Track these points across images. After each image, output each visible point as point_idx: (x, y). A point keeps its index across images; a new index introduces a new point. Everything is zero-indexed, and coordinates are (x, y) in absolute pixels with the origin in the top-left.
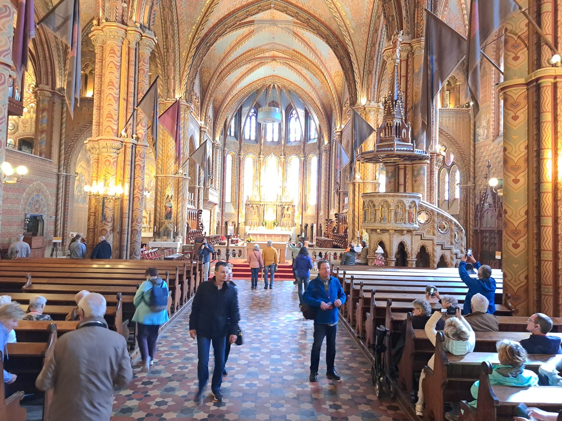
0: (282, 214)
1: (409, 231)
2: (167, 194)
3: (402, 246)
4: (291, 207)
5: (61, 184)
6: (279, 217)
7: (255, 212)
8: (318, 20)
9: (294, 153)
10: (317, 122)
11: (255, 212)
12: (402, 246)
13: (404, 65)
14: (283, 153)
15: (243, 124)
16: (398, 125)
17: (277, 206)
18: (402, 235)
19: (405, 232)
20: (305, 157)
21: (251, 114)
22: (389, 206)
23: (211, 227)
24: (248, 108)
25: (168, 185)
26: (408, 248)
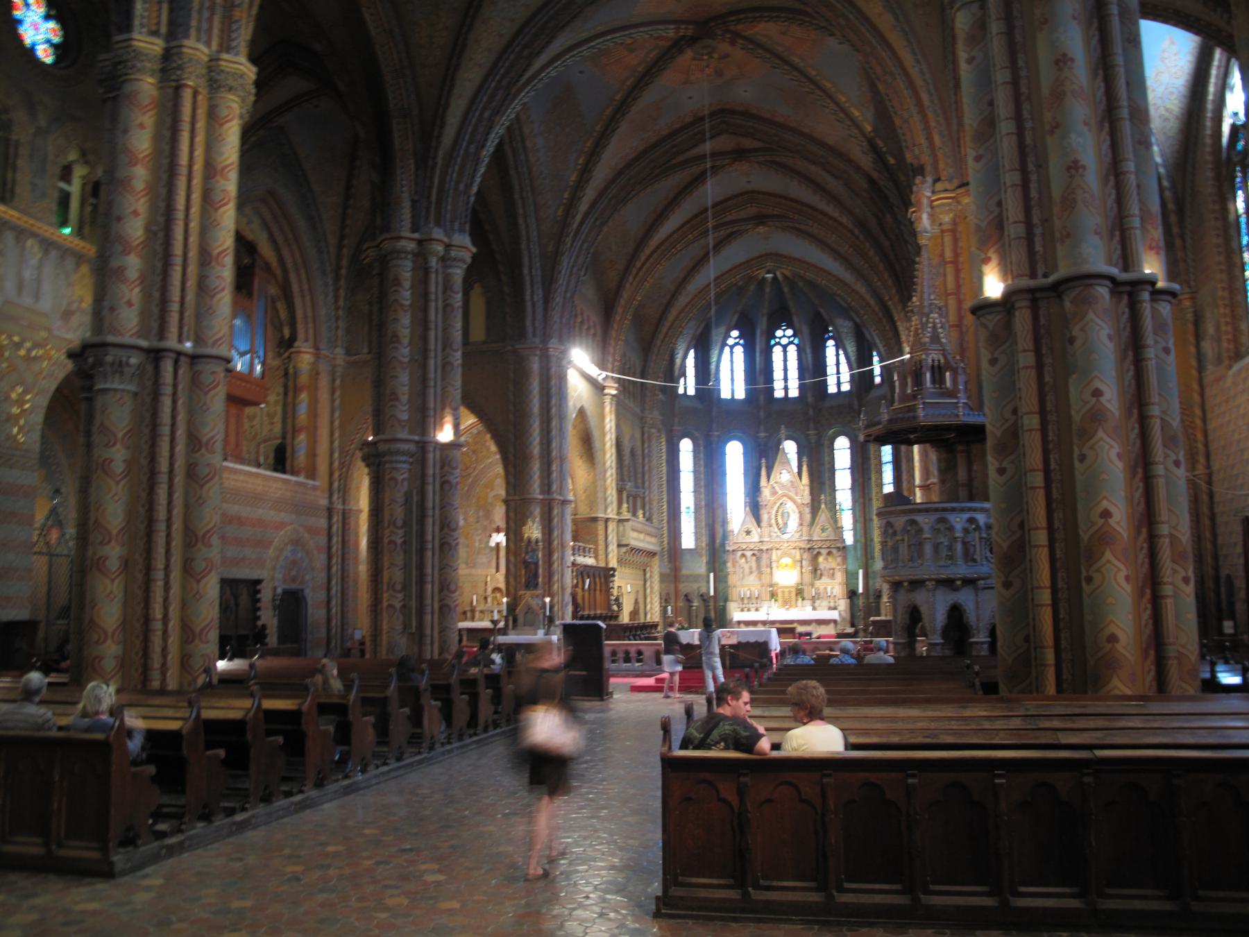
1: (969, 582)
2: (526, 536)
3: (956, 612)
4: (834, 551)
5: (334, 528)
6: (808, 577)
7: (751, 568)
8: (823, 144)
10: (882, 350)
12: (956, 612)
13: (948, 239)
15: (713, 367)
16: (936, 363)
18: (956, 589)
19: (959, 583)
21: (730, 342)
22: (920, 531)
23: (648, 607)
24: (722, 330)
25: (528, 518)
26: (971, 616)
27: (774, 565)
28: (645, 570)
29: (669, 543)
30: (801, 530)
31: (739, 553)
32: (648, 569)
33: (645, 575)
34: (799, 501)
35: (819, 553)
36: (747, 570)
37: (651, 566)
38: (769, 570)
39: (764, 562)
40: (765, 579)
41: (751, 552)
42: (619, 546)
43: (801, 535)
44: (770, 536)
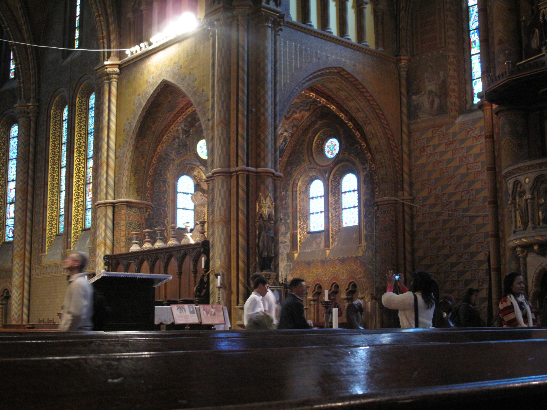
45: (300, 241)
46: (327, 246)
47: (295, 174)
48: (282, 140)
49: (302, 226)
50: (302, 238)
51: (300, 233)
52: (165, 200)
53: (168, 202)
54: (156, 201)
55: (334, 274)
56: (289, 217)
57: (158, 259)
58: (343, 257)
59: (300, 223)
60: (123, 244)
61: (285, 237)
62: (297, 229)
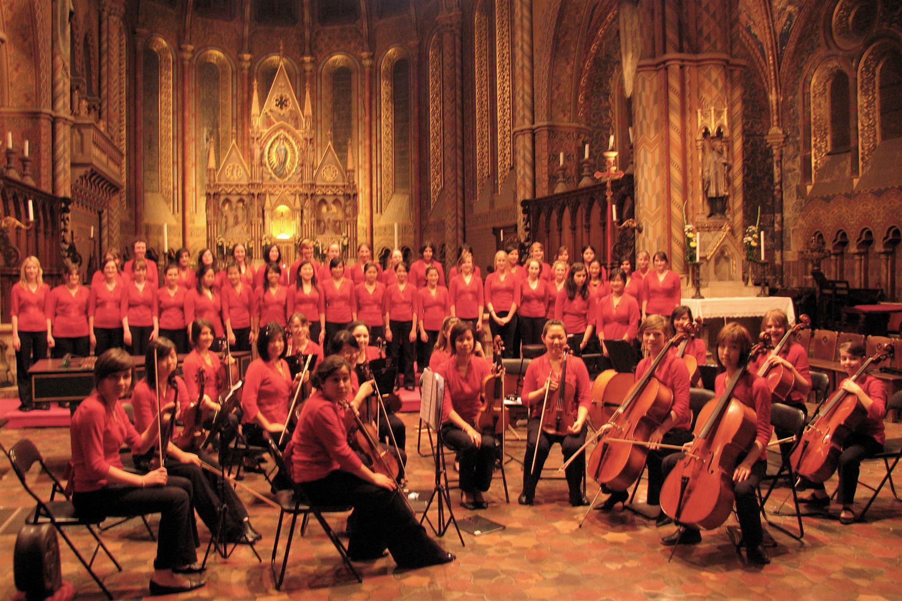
0: (319, 222)
4: (342, 199)
7: (236, 217)
9: (342, 47)
11: (236, 217)
14: (307, 49)
17: (303, 198)
20: (372, 57)
27: (267, 214)
28: (100, 213)
29: (128, 181)
30: (302, 171)
31: (222, 198)
32: (105, 211)
33: (100, 219)
34: (301, 136)
35: (323, 201)
36: (231, 221)
37: (109, 208)
38: (261, 221)
39: (255, 210)
40: (256, 231)
41: (237, 198)
42: (74, 165)
43: (302, 178)
44: (262, 178)
45: (816, 167)
46: (855, 172)
47: (806, 69)
48: (784, 19)
49: (819, 145)
50: (819, 162)
51: (815, 155)
52: (608, 120)
53: (613, 122)
54: (595, 122)
55: (865, 215)
56: (798, 132)
57: (579, 204)
58: (879, 189)
59: (815, 141)
60: (545, 184)
61: (793, 162)
62: (811, 151)
